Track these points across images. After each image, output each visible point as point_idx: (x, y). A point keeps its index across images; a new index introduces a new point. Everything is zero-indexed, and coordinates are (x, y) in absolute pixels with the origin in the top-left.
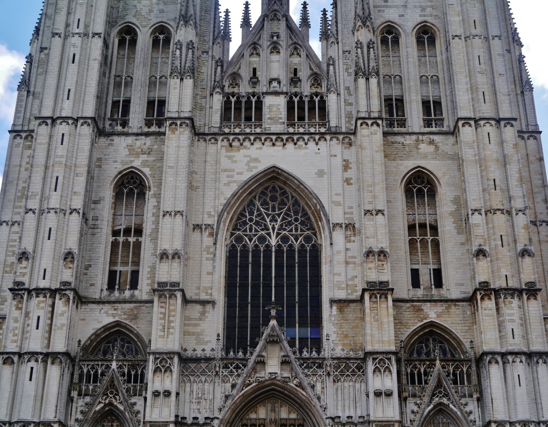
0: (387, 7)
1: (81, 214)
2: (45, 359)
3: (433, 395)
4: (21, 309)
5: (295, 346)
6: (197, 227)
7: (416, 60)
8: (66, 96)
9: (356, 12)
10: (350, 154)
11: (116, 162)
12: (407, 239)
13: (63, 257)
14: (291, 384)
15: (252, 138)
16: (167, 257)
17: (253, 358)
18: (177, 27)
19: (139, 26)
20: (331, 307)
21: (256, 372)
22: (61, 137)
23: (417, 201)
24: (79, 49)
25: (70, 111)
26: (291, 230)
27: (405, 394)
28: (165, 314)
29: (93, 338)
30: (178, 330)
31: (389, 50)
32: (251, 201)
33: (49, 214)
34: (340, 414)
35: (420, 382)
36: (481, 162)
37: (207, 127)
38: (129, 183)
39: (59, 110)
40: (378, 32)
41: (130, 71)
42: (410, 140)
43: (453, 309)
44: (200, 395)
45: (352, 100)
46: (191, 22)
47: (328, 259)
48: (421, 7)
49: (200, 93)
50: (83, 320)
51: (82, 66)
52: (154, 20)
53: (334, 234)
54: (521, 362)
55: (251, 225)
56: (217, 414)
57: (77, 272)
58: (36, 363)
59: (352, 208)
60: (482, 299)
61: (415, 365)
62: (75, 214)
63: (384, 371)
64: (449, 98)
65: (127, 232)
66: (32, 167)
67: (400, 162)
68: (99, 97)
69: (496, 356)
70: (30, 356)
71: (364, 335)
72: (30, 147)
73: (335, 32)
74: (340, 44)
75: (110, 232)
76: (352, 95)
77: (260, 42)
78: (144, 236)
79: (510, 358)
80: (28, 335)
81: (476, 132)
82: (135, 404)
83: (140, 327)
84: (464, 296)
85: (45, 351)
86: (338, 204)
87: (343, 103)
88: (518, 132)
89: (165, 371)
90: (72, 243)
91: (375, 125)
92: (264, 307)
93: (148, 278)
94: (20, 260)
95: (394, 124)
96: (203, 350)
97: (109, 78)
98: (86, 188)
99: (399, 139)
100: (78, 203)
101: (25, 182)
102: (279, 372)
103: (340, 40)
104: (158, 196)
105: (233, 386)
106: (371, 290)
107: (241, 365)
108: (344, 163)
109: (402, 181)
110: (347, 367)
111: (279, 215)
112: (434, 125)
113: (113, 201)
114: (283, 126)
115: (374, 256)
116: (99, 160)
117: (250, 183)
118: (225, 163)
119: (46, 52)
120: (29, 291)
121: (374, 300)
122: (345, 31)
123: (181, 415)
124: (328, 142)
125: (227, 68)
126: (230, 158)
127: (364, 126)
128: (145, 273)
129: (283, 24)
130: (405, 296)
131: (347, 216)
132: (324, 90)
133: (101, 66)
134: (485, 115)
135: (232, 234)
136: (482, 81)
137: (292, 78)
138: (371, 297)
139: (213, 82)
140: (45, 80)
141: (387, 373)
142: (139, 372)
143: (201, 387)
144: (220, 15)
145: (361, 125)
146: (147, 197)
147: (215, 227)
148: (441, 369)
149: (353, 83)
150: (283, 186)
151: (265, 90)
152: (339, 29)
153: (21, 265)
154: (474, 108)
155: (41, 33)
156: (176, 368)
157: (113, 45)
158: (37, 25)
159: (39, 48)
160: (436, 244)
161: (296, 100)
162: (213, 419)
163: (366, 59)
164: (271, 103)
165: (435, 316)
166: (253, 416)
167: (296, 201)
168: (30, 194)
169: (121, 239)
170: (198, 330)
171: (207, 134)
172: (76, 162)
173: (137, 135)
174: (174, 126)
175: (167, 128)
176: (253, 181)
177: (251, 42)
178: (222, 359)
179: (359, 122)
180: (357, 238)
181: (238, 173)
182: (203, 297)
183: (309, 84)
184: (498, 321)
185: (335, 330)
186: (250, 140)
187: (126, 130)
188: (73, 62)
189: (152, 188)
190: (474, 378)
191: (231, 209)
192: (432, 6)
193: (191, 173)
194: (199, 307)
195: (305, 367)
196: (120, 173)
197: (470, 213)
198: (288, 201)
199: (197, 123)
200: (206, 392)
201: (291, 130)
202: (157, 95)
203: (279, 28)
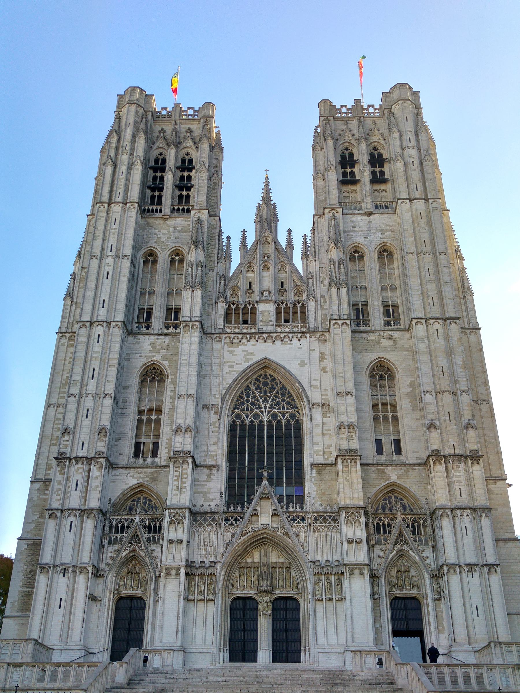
0: (355, 231)
1: (113, 397)
2: (82, 514)
3: (396, 543)
4: (63, 474)
5: (283, 502)
6: (206, 407)
7: (378, 273)
8: (101, 305)
9: (329, 235)
10: (327, 349)
11: (141, 356)
12: (372, 415)
13: (98, 431)
14: (280, 533)
15: (248, 336)
16: (181, 431)
18: (189, 251)
19: (159, 249)
20: (312, 470)
21: (251, 524)
22: (97, 337)
23: (380, 385)
24: (112, 268)
25: (105, 317)
26: (279, 409)
27: (373, 542)
28: (178, 477)
29: (121, 497)
30: (189, 489)
31: (356, 266)
32: (248, 386)
33: (87, 398)
34: (320, 559)
35: (385, 532)
37: (213, 328)
38: (151, 372)
39: (96, 315)
40: (348, 252)
41: (153, 285)
42: (373, 337)
43: (411, 472)
44: (206, 543)
45: (326, 305)
46: (200, 246)
47: (309, 431)
48: (382, 230)
49: (207, 302)
50: (113, 482)
51: (114, 281)
52: (171, 245)
53: (314, 411)
54: (468, 515)
55: (248, 405)
56: (219, 558)
57: (109, 444)
58: (74, 518)
59: (327, 390)
60: (434, 463)
61: (380, 518)
62: (108, 398)
63: (355, 523)
64: (404, 303)
65: (150, 411)
66: (74, 360)
67: (366, 354)
68: (128, 306)
69: (447, 511)
70: (70, 512)
71: (339, 493)
72: (72, 345)
73: (314, 253)
74: (317, 262)
75: (137, 412)
76: (326, 302)
78: (163, 414)
79: (458, 512)
80: (69, 495)
81: (427, 329)
82: (154, 550)
83: (158, 488)
84: (419, 461)
85: (82, 508)
86: (316, 387)
87: (319, 308)
88: (462, 328)
89: (179, 523)
90: (106, 420)
91: (345, 325)
92: (258, 470)
93: (166, 448)
94: (63, 434)
95: (360, 324)
96: (210, 505)
97: (136, 290)
98: (117, 377)
99: (364, 335)
100: (110, 389)
101: (68, 373)
102: (270, 524)
103: (317, 259)
104: (174, 382)
105: (233, 535)
106: (343, 456)
107: (239, 518)
108: (321, 355)
109: (367, 369)
110: (325, 519)
111: (270, 397)
112: (392, 324)
113: (139, 387)
114: (272, 327)
115: (345, 428)
116: (128, 355)
117: (247, 371)
118: (227, 356)
119: (86, 270)
121: (345, 464)
122: (321, 251)
123: (191, 560)
124: (308, 339)
125: (229, 282)
126: (231, 352)
127: (336, 326)
128: (164, 443)
129: (272, 246)
130: (370, 461)
131: (323, 397)
132: (305, 298)
133: (129, 281)
134: (433, 315)
135: (233, 413)
136: (431, 288)
137: (280, 289)
138: (343, 462)
139: (218, 293)
140: (85, 292)
141: (357, 524)
142: (158, 525)
143: (207, 536)
144: (223, 240)
145: (334, 325)
146: (166, 383)
147: (219, 407)
148: (402, 522)
149: (327, 293)
150: (272, 373)
151: (258, 299)
152: (317, 250)
153: (64, 439)
154: (424, 310)
155: (82, 255)
156: (186, 521)
157: (139, 264)
158: (79, 250)
159: (80, 268)
160: (395, 419)
161: (282, 306)
162: (215, 563)
163: (337, 273)
164: (263, 309)
165: (396, 477)
166: (249, 560)
167: (283, 386)
168: (72, 382)
169: (145, 417)
170: (205, 489)
171: (213, 334)
172: (109, 356)
173: (158, 335)
174: (187, 328)
175: (182, 330)
176: (249, 370)
177: (247, 262)
178: (224, 513)
179: (332, 323)
180: (332, 414)
181: (238, 364)
182: (210, 462)
183: (293, 293)
184: (448, 482)
185: (315, 489)
186: (247, 338)
187: (149, 331)
188: (107, 278)
189: (170, 376)
190: (429, 529)
191: (232, 392)
192: (391, 230)
193: (200, 365)
194: (206, 471)
195: (291, 520)
196: (144, 365)
197: (423, 394)
198: (277, 385)
199: (205, 326)
200: (211, 540)
201: (279, 330)
202: (173, 304)
203: (269, 251)
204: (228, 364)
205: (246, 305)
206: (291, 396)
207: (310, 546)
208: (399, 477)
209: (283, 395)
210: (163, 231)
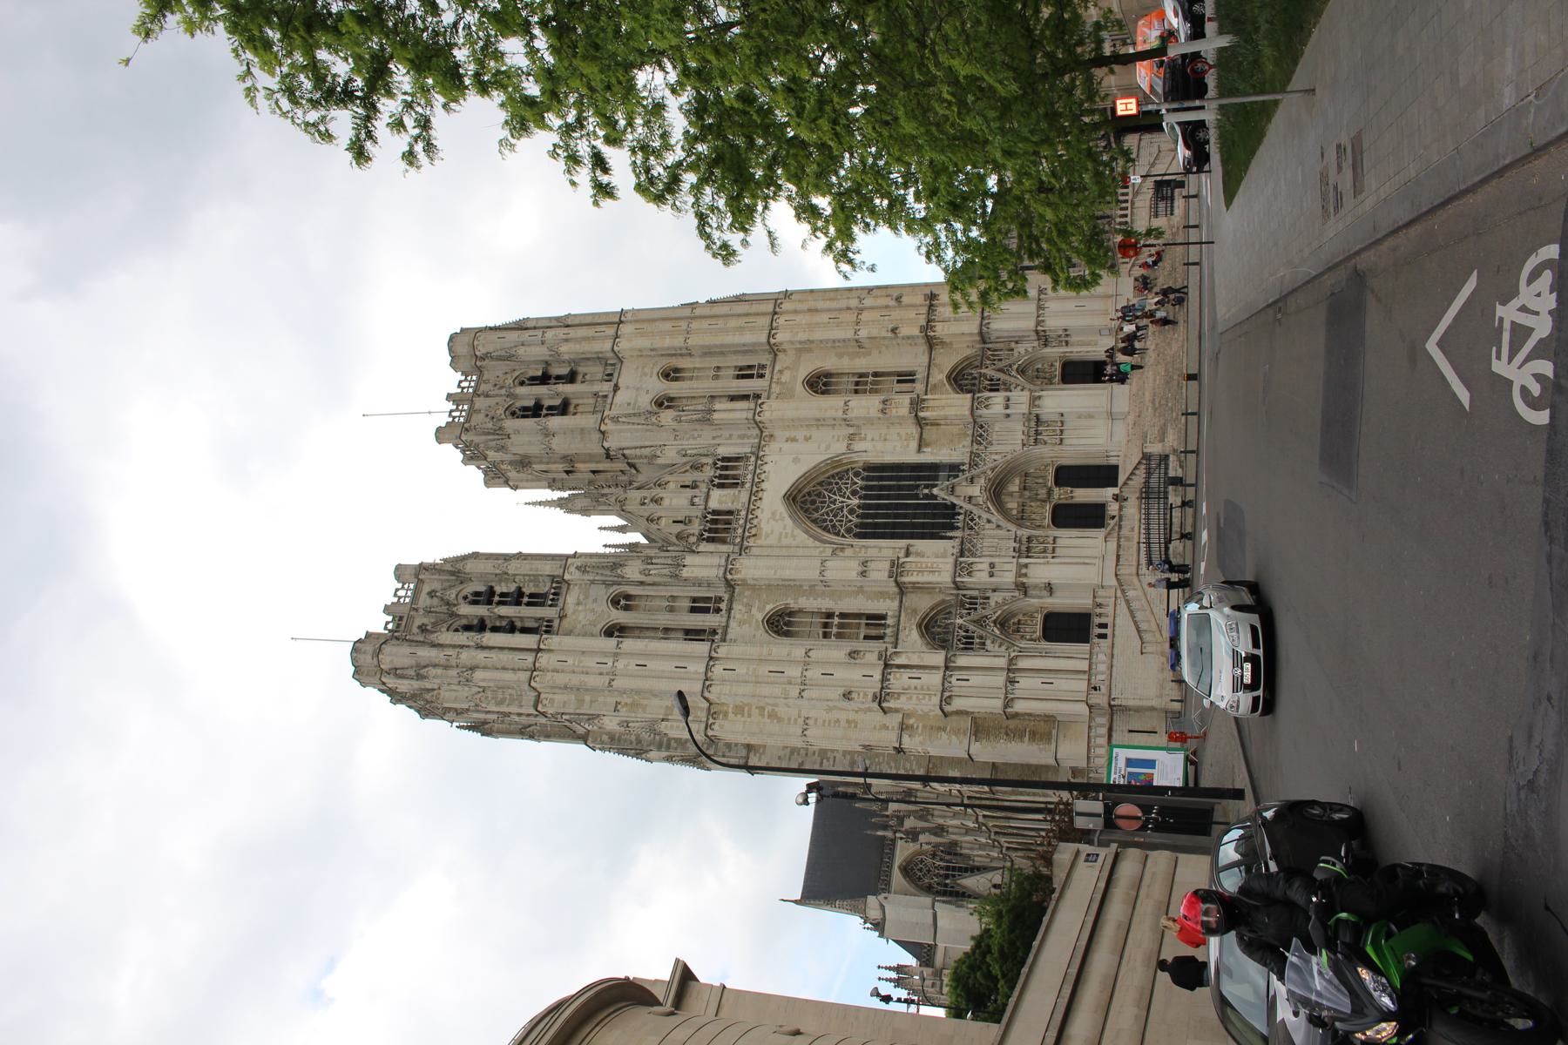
10: (781, 434)
17: (967, 506)
36: (811, 327)
59: (833, 437)
77: (647, 515)
85: (943, 669)
86: (828, 447)
87: (729, 441)
105: (989, 521)
111: (830, 498)
118: (772, 540)
120: (882, 688)
126: (767, 536)
135: (843, 536)
150: (801, 495)
160: (876, 374)
161: (717, 481)
166: (1015, 512)
178: (964, 530)
181: (785, 528)
201: (748, 485)
204: (783, 539)
205: (707, 522)
206: (833, 476)
207: (1008, 448)
208: (942, 372)
209: (830, 484)
210: (581, 617)
